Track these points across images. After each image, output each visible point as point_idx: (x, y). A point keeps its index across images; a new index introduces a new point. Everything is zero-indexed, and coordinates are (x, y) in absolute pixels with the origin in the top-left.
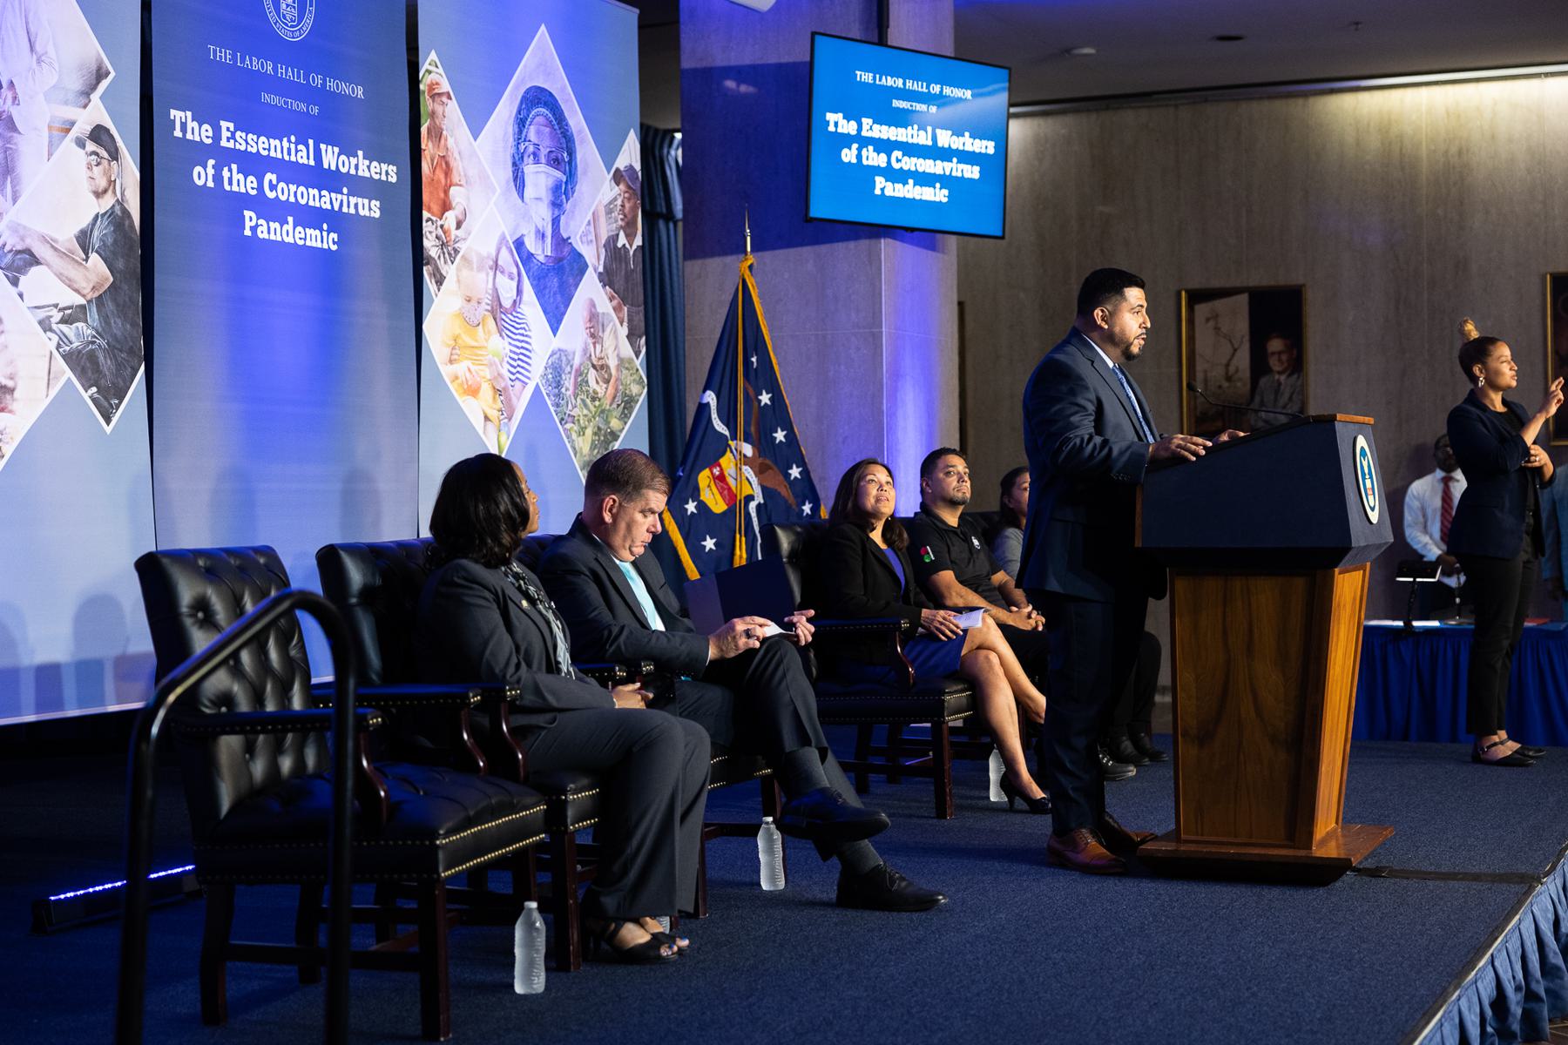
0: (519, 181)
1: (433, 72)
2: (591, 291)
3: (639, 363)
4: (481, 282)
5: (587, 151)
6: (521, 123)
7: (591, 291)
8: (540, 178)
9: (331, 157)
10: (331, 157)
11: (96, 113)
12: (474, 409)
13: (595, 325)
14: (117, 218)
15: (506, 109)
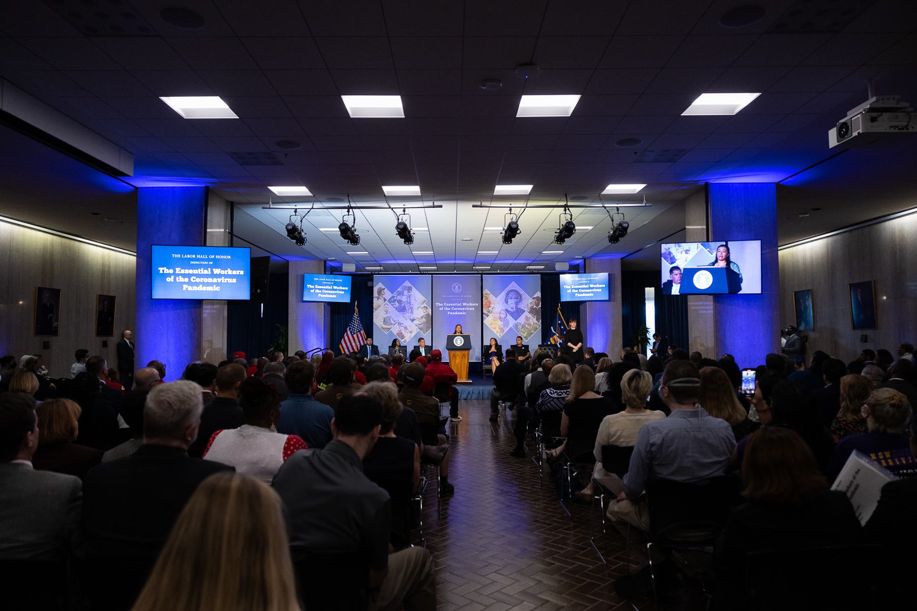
0: (506, 302)
1: (486, 291)
2: (526, 314)
3: (540, 323)
4: (498, 315)
5: (525, 296)
6: (507, 295)
7: (526, 314)
8: (512, 302)
9: (464, 304)
10: (464, 304)
11: (425, 305)
12: (495, 331)
13: (527, 319)
14: (428, 315)
15: (503, 294)
